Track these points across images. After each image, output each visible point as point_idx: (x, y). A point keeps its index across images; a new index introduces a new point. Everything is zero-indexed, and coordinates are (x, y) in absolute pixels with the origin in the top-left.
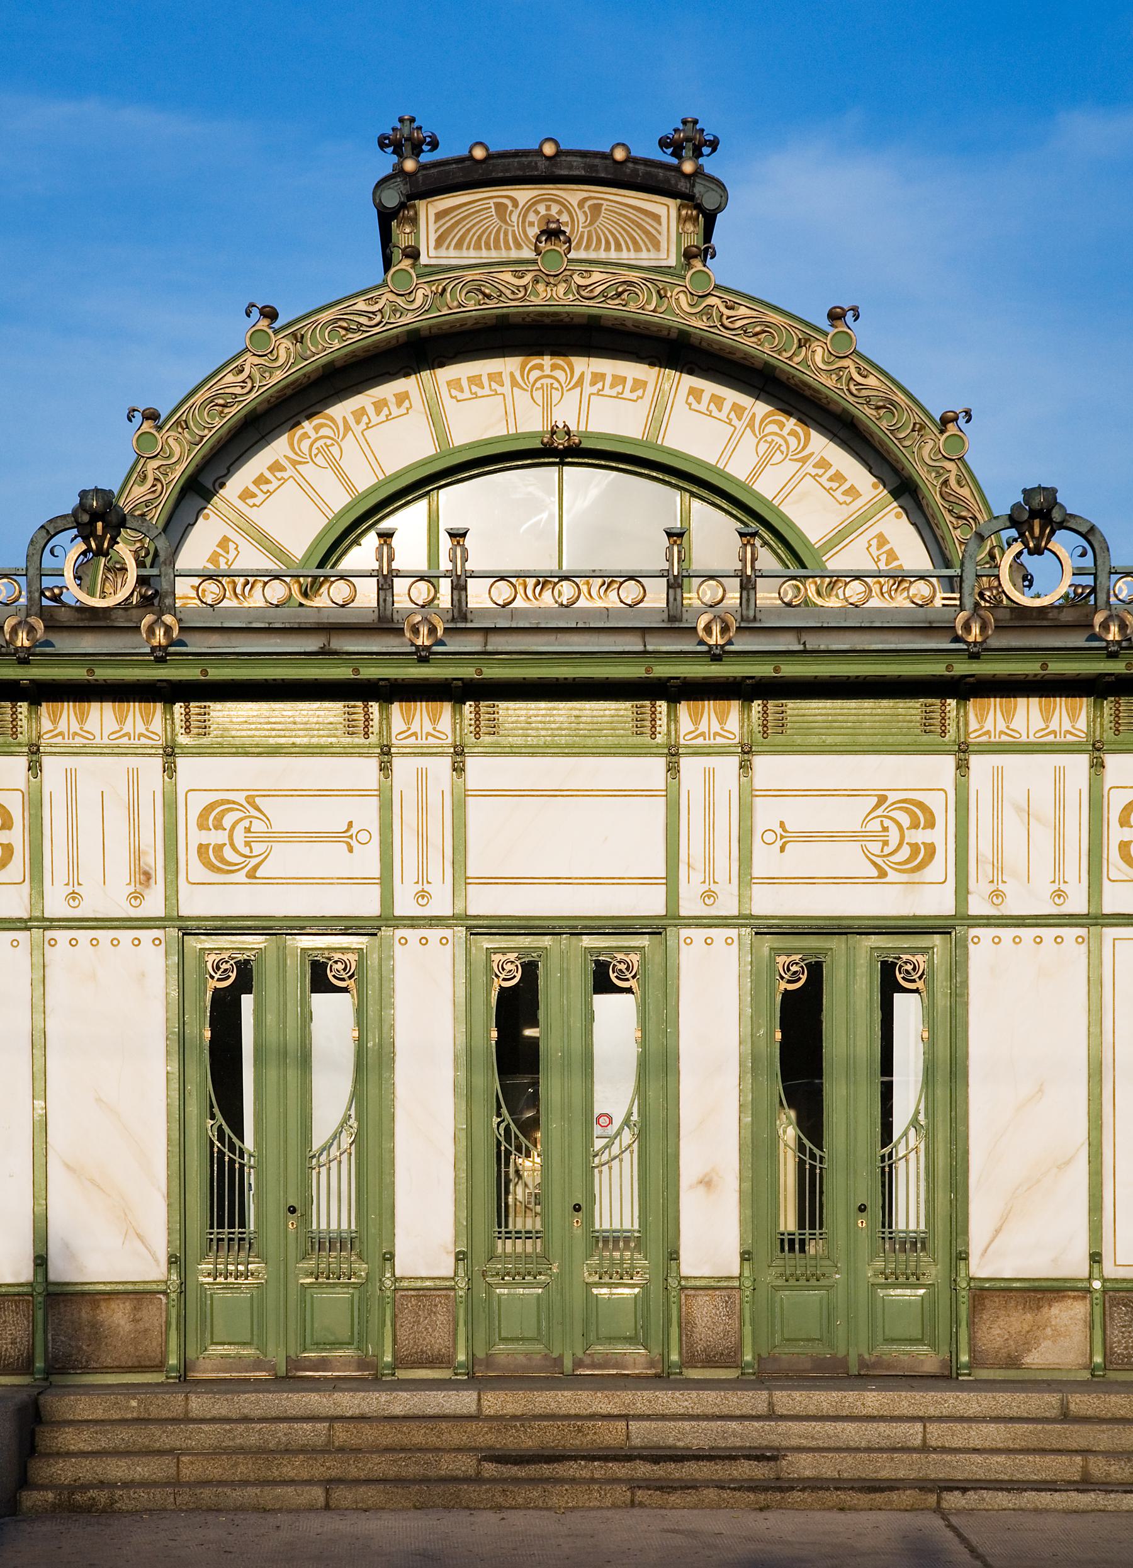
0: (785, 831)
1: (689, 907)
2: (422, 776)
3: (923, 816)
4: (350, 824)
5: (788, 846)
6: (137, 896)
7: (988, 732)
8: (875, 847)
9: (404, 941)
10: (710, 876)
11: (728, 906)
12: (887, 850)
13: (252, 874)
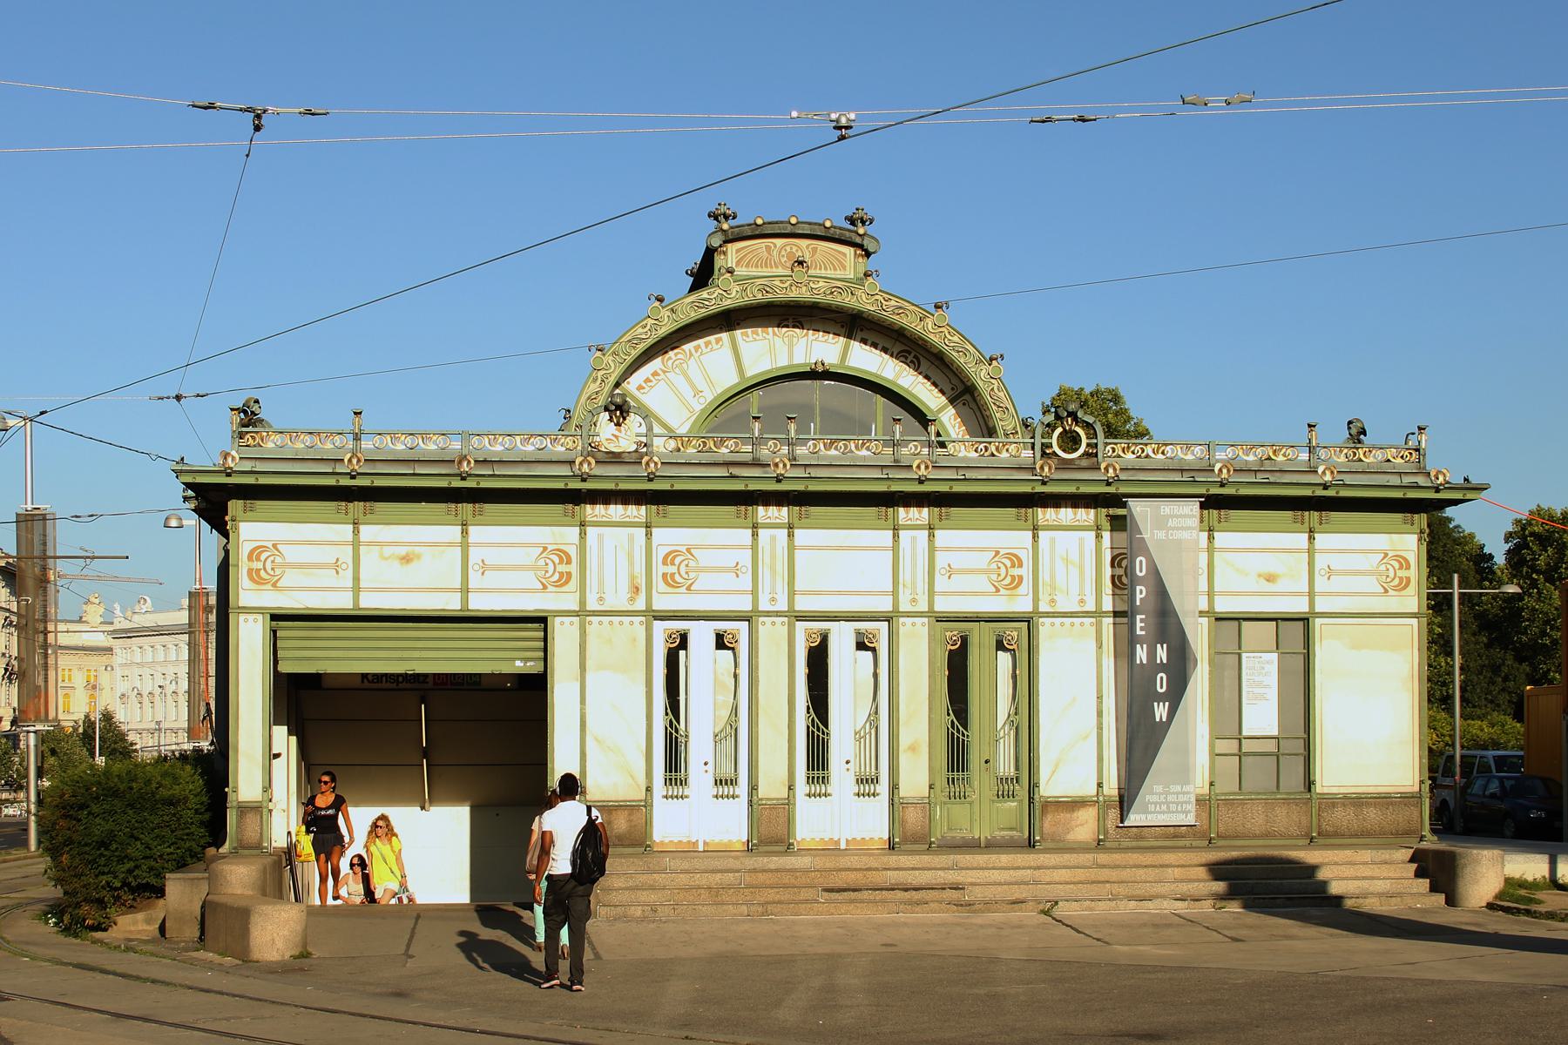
1: (904, 606)
2: (773, 539)
3: (1017, 561)
6: (632, 599)
9: (764, 623)
10: (914, 592)
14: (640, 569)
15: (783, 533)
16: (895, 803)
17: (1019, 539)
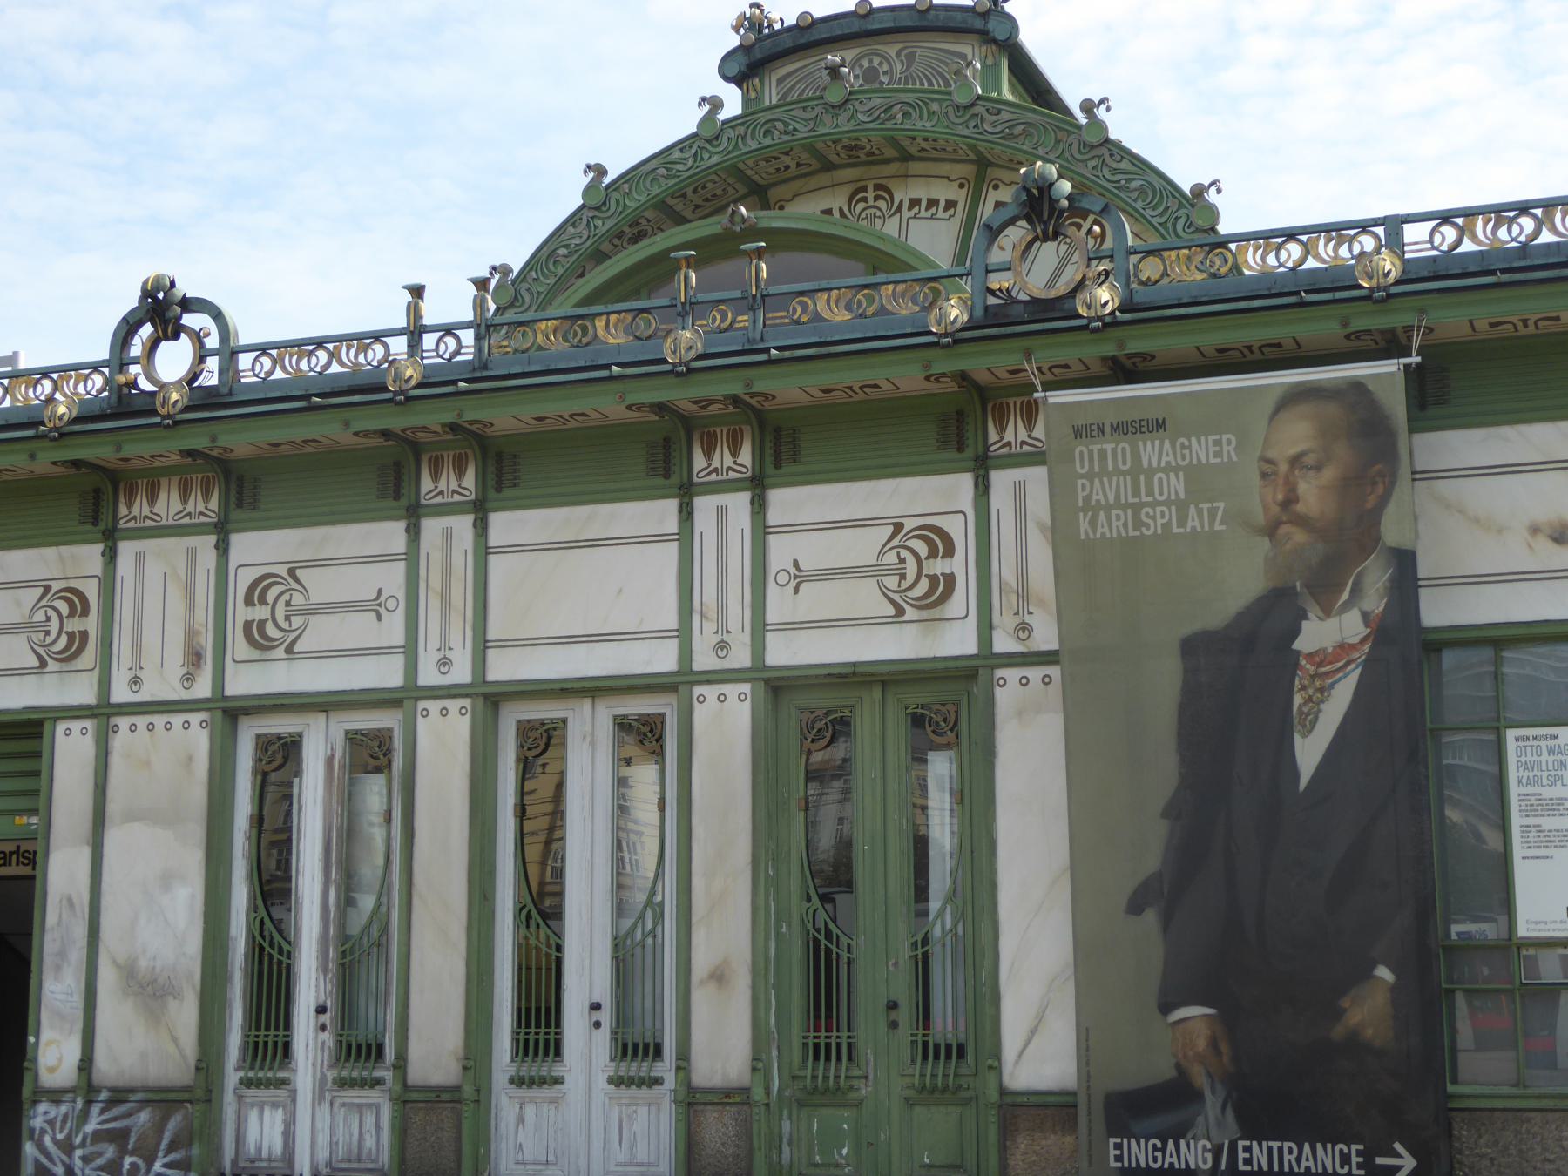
0: (798, 569)
1: (704, 660)
3: (941, 543)
4: (380, 591)
5: (803, 587)
6: (189, 678)
7: (1009, 444)
8: (892, 582)
11: (741, 657)
12: (905, 585)
13: (289, 649)
14: (204, 615)
15: (463, 525)
16: (692, 1101)
17: (941, 495)
